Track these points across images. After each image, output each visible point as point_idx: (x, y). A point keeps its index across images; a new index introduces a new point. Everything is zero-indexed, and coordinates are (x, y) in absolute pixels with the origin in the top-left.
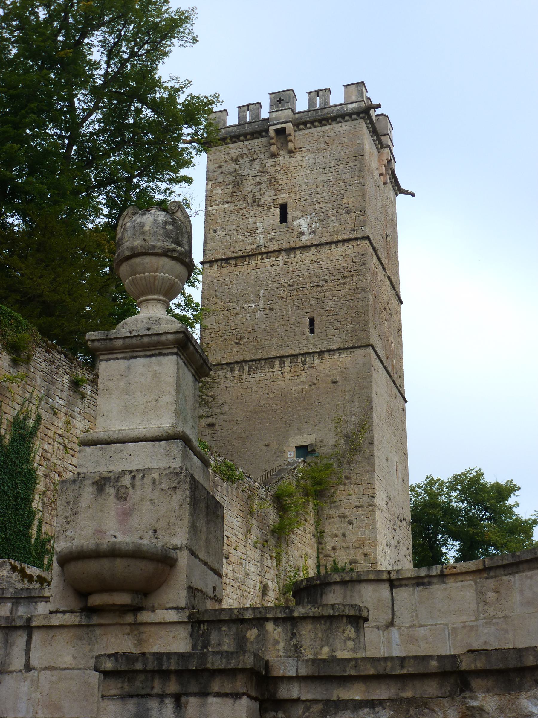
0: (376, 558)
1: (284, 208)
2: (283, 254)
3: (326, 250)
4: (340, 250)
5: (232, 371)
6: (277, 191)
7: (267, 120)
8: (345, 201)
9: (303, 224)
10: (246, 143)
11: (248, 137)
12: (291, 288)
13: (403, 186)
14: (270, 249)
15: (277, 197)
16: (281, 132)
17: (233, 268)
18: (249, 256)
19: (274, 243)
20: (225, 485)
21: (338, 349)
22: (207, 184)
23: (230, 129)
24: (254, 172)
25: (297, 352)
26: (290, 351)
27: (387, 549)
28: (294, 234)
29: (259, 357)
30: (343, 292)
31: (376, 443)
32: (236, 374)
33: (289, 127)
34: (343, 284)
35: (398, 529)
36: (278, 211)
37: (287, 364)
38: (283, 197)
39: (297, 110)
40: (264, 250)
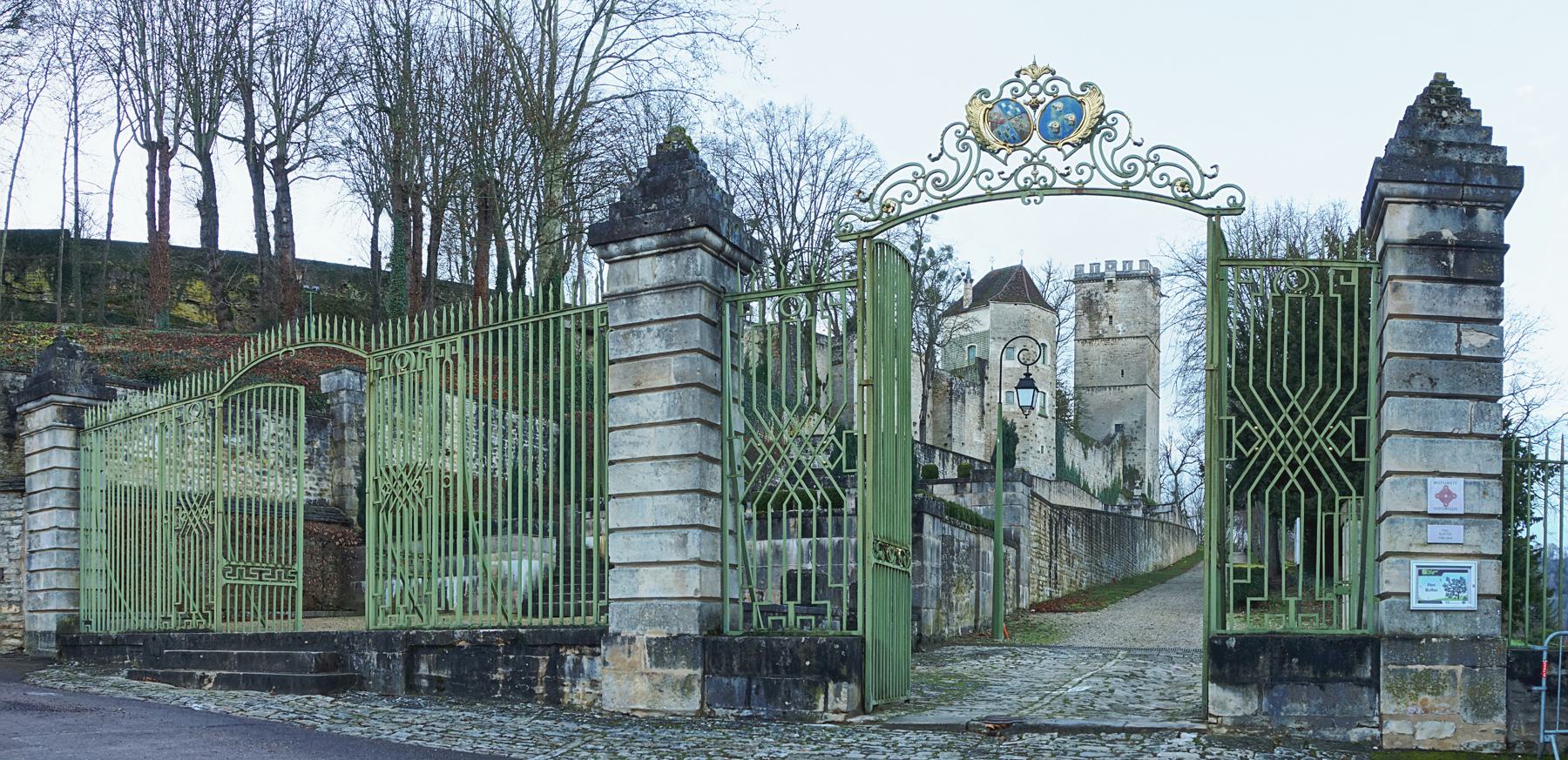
3: (1129, 340)
4: (1135, 341)
9: (1120, 327)
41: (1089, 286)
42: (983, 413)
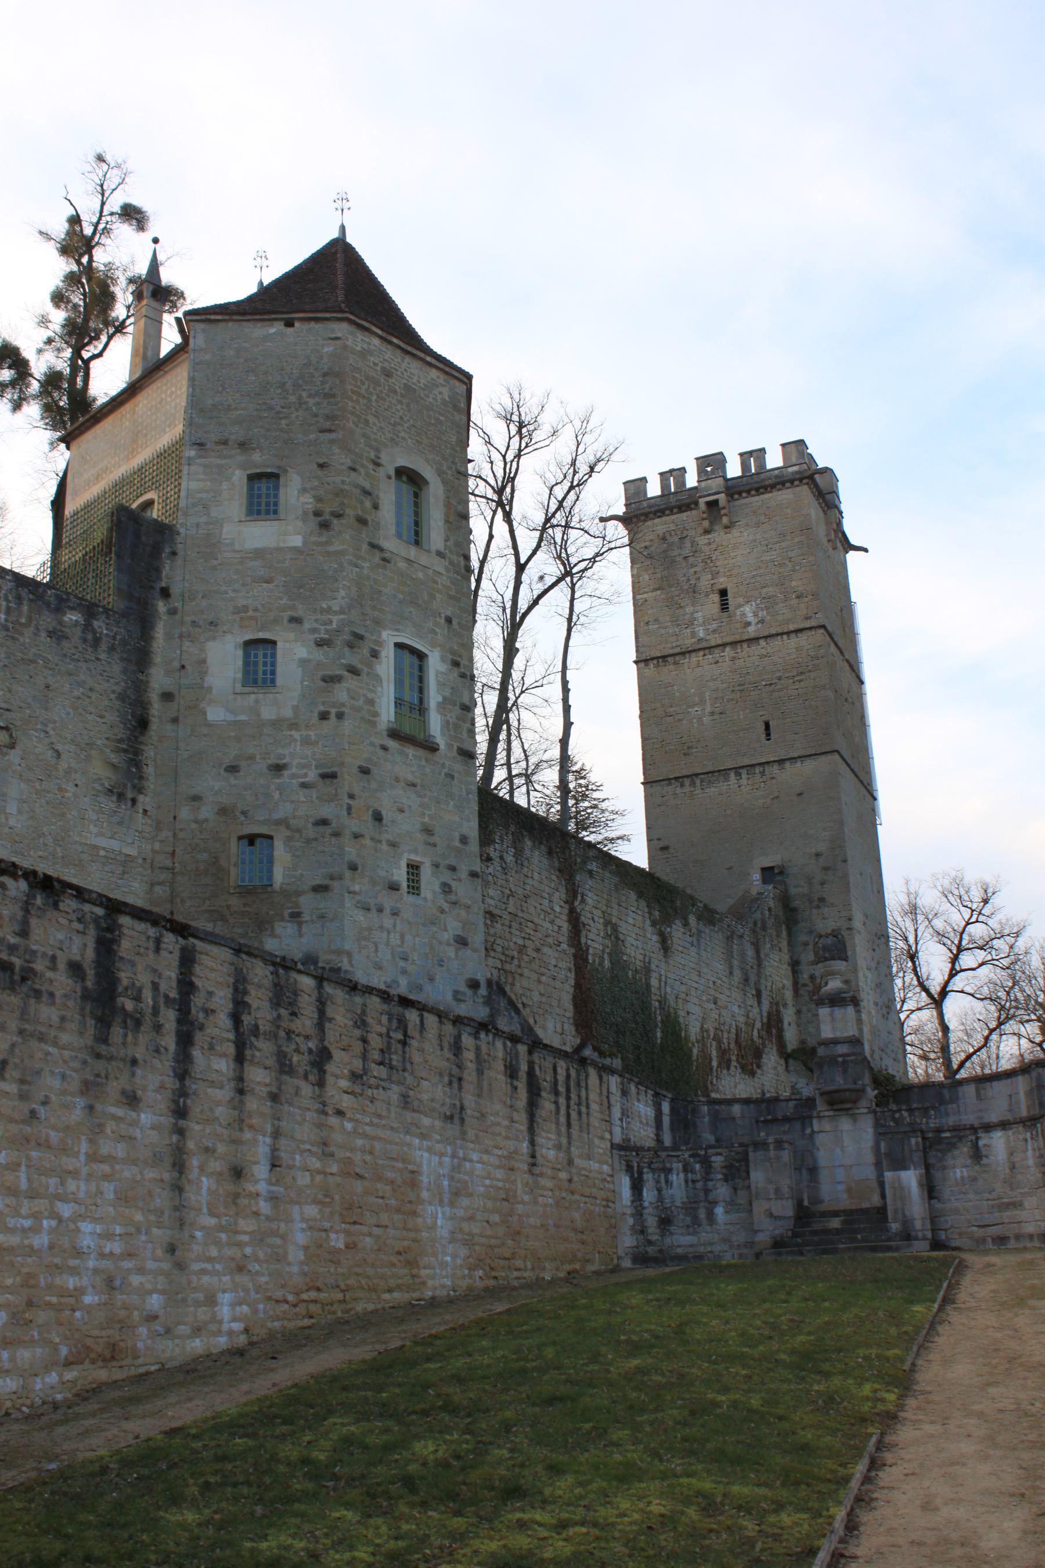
0: (857, 985)
1: (723, 593)
2: (728, 649)
3: (777, 642)
4: (793, 642)
5: (682, 785)
6: (715, 575)
7: (695, 488)
8: (794, 584)
9: (748, 611)
10: (673, 517)
11: (675, 510)
12: (741, 688)
13: (853, 541)
14: (713, 644)
15: (715, 581)
16: (713, 505)
17: (672, 667)
18: (690, 652)
19: (717, 636)
20: (707, 931)
21: (800, 757)
22: (632, 567)
23: (653, 501)
24: (686, 552)
25: (754, 762)
26: (747, 761)
27: (867, 973)
28: (738, 625)
29: (711, 769)
30: (800, 691)
31: (849, 859)
32: (687, 789)
33: (722, 497)
34: (800, 681)
35: (877, 949)
36: (716, 598)
37: (744, 776)
38: (722, 582)
39: (729, 476)
40: (704, 644)
41: (660, 526)
42: (143, 724)
